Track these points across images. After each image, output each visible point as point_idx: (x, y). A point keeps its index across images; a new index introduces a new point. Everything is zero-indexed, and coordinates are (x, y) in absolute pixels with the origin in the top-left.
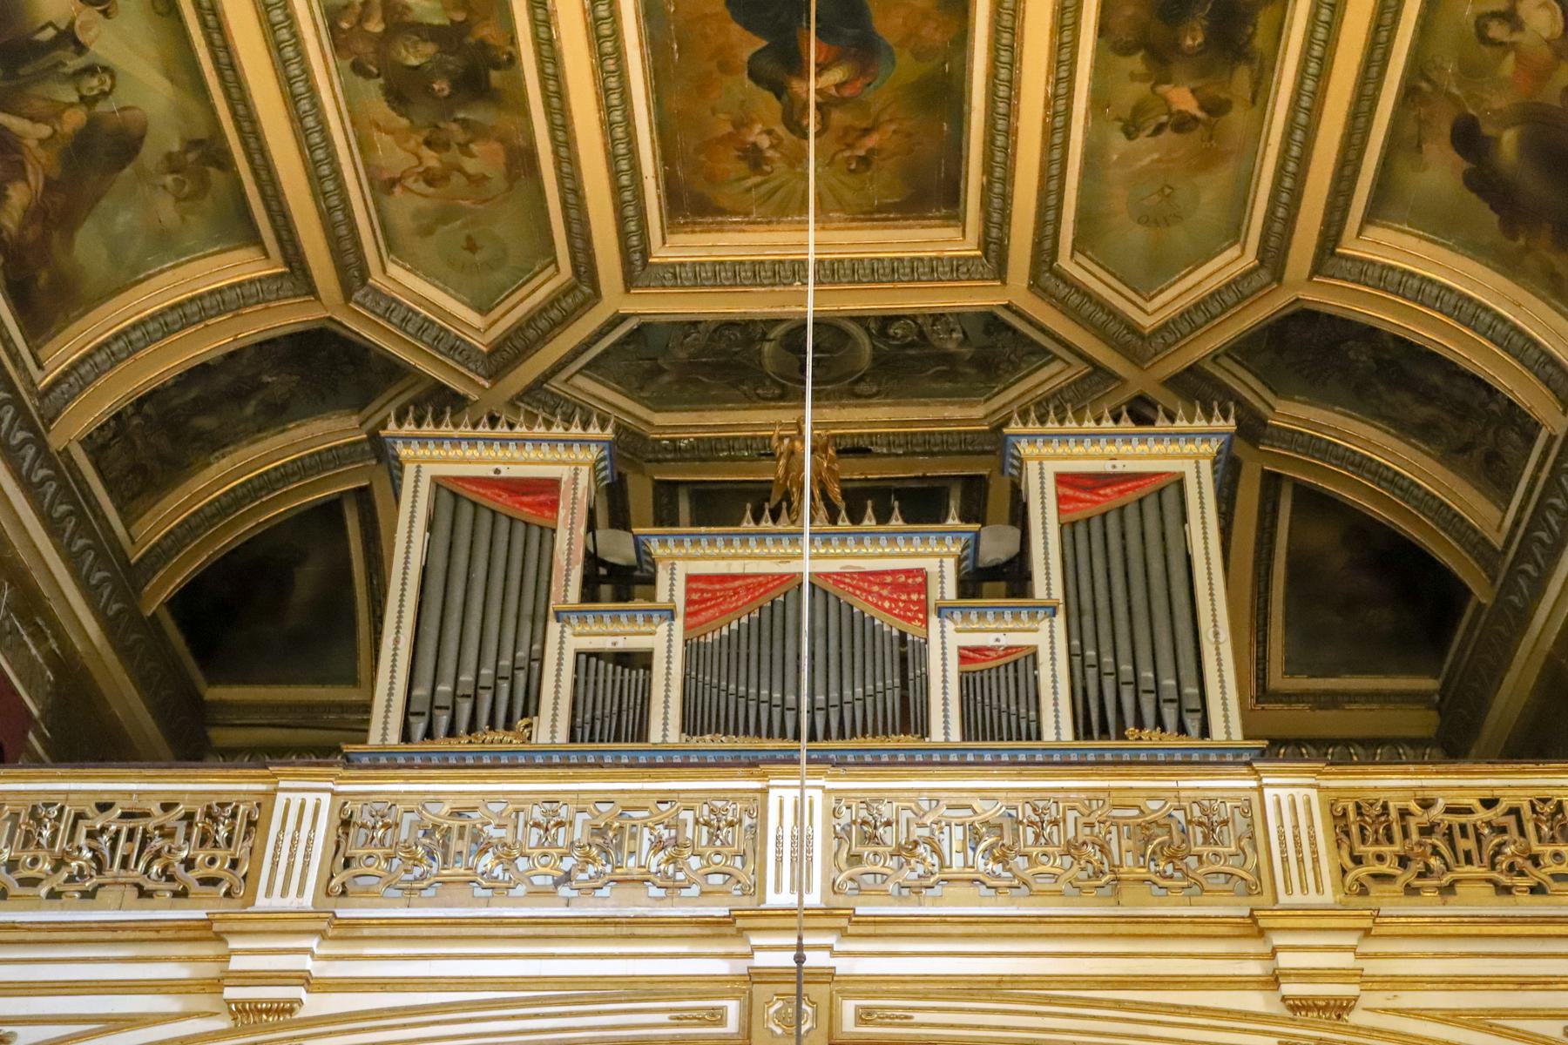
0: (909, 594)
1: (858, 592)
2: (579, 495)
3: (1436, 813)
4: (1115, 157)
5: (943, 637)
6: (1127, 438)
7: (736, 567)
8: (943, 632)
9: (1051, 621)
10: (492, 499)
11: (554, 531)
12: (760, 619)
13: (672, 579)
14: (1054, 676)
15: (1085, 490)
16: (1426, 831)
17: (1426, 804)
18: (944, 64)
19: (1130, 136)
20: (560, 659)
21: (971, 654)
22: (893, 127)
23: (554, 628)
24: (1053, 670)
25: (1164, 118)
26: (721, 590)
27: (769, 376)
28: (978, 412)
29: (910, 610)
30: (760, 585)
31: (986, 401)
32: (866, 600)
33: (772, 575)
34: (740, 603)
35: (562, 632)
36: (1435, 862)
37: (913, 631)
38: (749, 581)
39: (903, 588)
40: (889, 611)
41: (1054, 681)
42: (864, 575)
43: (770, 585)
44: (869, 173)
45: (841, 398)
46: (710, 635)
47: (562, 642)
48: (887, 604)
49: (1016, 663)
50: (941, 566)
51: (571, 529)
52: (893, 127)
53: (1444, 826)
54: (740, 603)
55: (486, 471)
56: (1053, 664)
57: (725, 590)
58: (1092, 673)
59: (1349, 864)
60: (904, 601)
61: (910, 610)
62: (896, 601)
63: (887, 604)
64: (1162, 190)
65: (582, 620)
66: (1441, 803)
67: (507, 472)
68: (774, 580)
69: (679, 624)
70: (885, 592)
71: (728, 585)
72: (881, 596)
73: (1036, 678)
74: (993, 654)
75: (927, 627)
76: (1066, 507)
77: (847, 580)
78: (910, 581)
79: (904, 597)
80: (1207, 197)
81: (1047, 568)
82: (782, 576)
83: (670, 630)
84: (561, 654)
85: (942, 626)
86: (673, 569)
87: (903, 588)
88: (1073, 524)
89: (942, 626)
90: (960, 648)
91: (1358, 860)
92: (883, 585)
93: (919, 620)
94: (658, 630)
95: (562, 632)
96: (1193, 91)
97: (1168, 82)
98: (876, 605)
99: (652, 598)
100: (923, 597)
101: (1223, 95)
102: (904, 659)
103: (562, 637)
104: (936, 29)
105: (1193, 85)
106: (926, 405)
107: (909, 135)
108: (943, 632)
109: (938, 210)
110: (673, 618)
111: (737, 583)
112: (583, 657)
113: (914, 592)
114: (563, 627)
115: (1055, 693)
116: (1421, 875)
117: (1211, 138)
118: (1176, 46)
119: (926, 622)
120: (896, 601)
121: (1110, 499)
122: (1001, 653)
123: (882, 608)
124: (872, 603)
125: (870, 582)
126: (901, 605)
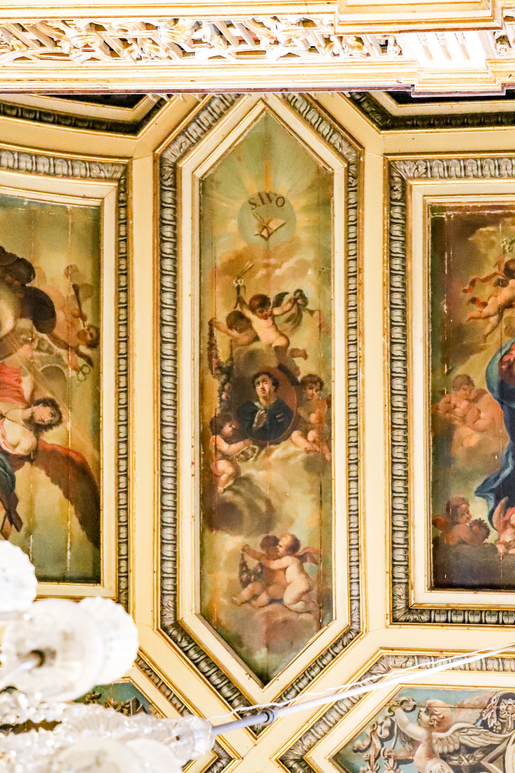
4: (310, 272)
18: (449, 373)
19: (300, 294)
22: (486, 310)
25: (277, 311)
44: (507, 259)
52: (486, 310)
64: (269, 235)
80: (233, 225)
96: (257, 338)
97: (277, 348)
101: (235, 333)
104: (455, 407)
105: (256, 346)
107: (474, 300)
109: (449, 217)
117: (238, 288)
118: (276, 384)
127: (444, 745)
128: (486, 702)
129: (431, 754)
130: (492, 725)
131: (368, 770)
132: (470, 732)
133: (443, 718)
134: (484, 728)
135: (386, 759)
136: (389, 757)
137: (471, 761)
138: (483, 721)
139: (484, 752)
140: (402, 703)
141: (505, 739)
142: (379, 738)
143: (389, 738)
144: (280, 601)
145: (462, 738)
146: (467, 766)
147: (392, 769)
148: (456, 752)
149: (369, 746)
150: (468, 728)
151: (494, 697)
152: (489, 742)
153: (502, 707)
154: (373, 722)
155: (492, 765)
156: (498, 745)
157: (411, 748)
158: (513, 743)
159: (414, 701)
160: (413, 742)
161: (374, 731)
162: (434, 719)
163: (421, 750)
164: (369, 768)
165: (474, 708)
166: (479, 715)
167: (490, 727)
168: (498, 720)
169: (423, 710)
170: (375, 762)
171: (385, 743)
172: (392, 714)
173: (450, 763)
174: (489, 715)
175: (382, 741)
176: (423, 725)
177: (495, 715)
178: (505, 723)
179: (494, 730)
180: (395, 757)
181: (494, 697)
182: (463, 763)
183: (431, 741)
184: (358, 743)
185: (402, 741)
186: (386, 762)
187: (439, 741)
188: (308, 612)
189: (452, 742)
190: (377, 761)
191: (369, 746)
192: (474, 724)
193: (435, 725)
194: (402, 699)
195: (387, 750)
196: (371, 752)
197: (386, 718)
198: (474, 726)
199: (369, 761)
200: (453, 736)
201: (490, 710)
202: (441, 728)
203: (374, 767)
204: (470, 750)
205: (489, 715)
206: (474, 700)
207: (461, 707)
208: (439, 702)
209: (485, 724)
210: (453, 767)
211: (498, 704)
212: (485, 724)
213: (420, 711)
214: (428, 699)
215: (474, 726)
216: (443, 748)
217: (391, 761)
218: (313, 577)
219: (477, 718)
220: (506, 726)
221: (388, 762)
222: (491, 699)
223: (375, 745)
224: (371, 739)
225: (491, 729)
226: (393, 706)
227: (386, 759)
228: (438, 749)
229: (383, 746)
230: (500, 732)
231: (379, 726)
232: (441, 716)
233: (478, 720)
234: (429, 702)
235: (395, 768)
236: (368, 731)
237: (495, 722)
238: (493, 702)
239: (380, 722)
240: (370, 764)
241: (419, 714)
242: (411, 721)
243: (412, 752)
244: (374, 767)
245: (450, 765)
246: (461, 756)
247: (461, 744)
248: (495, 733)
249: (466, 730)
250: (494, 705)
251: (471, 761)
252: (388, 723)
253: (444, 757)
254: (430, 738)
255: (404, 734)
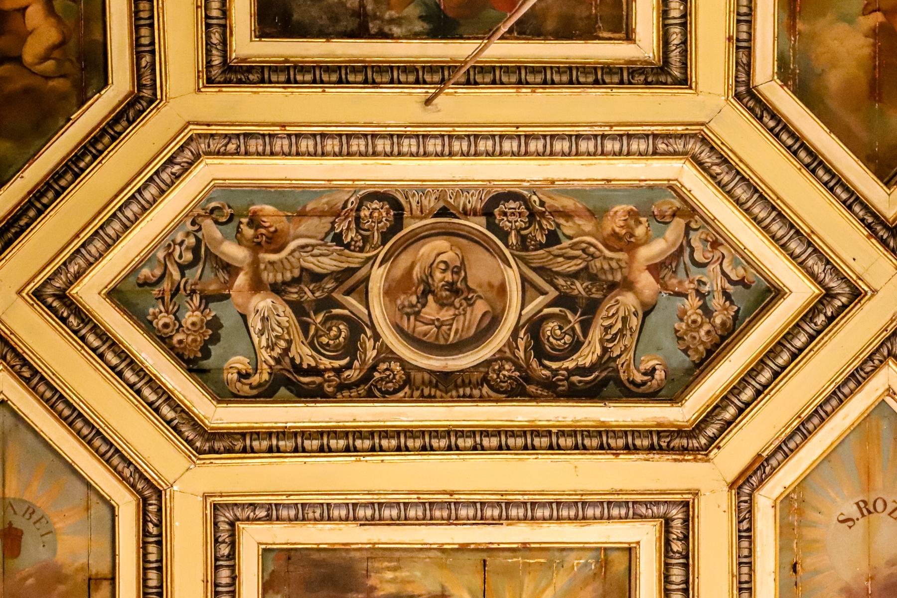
127: (277, 272)
128: (340, 205)
129: (257, 285)
130: (349, 240)
131: (161, 312)
132: (316, 251)
133: (276, 231)
134: (337, 245)
135: (189, 295)
136: (193, 292)
137: (317, 294)
138: (335, 234)
139: (336, 280)
140: (213, 210)
141: (369, 259)
142: (176, 262)
143: (193, 264)
144: (18, 60)
145: (304, 261)
146: (312, 301)
147: (198, 309)
148: (296, 281)
149: (163, 276)
150: (314, 246)
151: (352, 199)
152: (345, 265)
153: (365, 213)
154: (168, 240)
155: (349, 298)
156: (359, 268)
157: (227, 278)
158: (380, 266)
159: (230, 207)
160: (231, 270)
161: (170, 255)
162: (262, 234)
163: (242, 280)
164: (163, 309)
165: (321, 214)
166: (329, 226)
167: (345, 242)
168: (357, 232)
169: (245, 220)
170: (171, 300)
171: (187, 272)
172: (196, 228)
173: (285, 298)
174: (345, 225)
175: (182, 268)
176: (245, 242)
177: (353, 225)
178: (368, 236)
179: (352, 247)
180: (202, 291)
181: (352, 199)
182: (306, 297)
183: (258, 267)
184: (146, 272)
185: (212, 267)
186: (188, 299)
187: (269, 266)
188: (61, 76)
189: (288, 266)
190: (174, 300)
191: (163, 276)
192: (322, 240)
193: (263, 243)
194: (213, 204)
195: (190, 281)
196: (166, 285)
197: (188, 234)
198: (322, 242)
199: (162, 298)
200: (290, 257)
201: (346, 218)
202: (272, 247)
203: (171, 307)
204: (317, 278)
205: (345, 225)
206: (322, 203)
207: (303, 214)
208: (269, 209)
209: (338, 239)
210: (290, 303)
211: (358, 210)
212: (338, 239)
213: (241, 223)
214: (253, 204)
215: (320, 242)
216: (275, 276)
217: (196, 300)
218: (70, 23)
219: (326, 230)
220: (370, 240)
221: (192, 300)
222: (348, 200)
223: (171, 275)
224: (166, 266)
225: (348, 246)
226: (199, 215)
227: (189, 295)
228: (268, 277)
229: (183, 275)
230: (362, 250)
231: (177, 247)
232: (272, 229)
233: (327, 234)
234: (253, 208)
235: (202, 307)
236: (161, 254)
237: (353, 236)
238: (349, 206)
239: (179, 240)
240: (163, 305)
241: (239, 227)
242: (226, 237)
243: (229, 284)
244: (171, 307)
245: (286, 301)
246: (302, 286)
247: (303, 269)
248: (354, 251)
249: (309, 249)
250: (352, 210)
251: (317, 294)
252: (192, 240)
253: (277, 289)
254: (255, 263)
255: (216, 256)
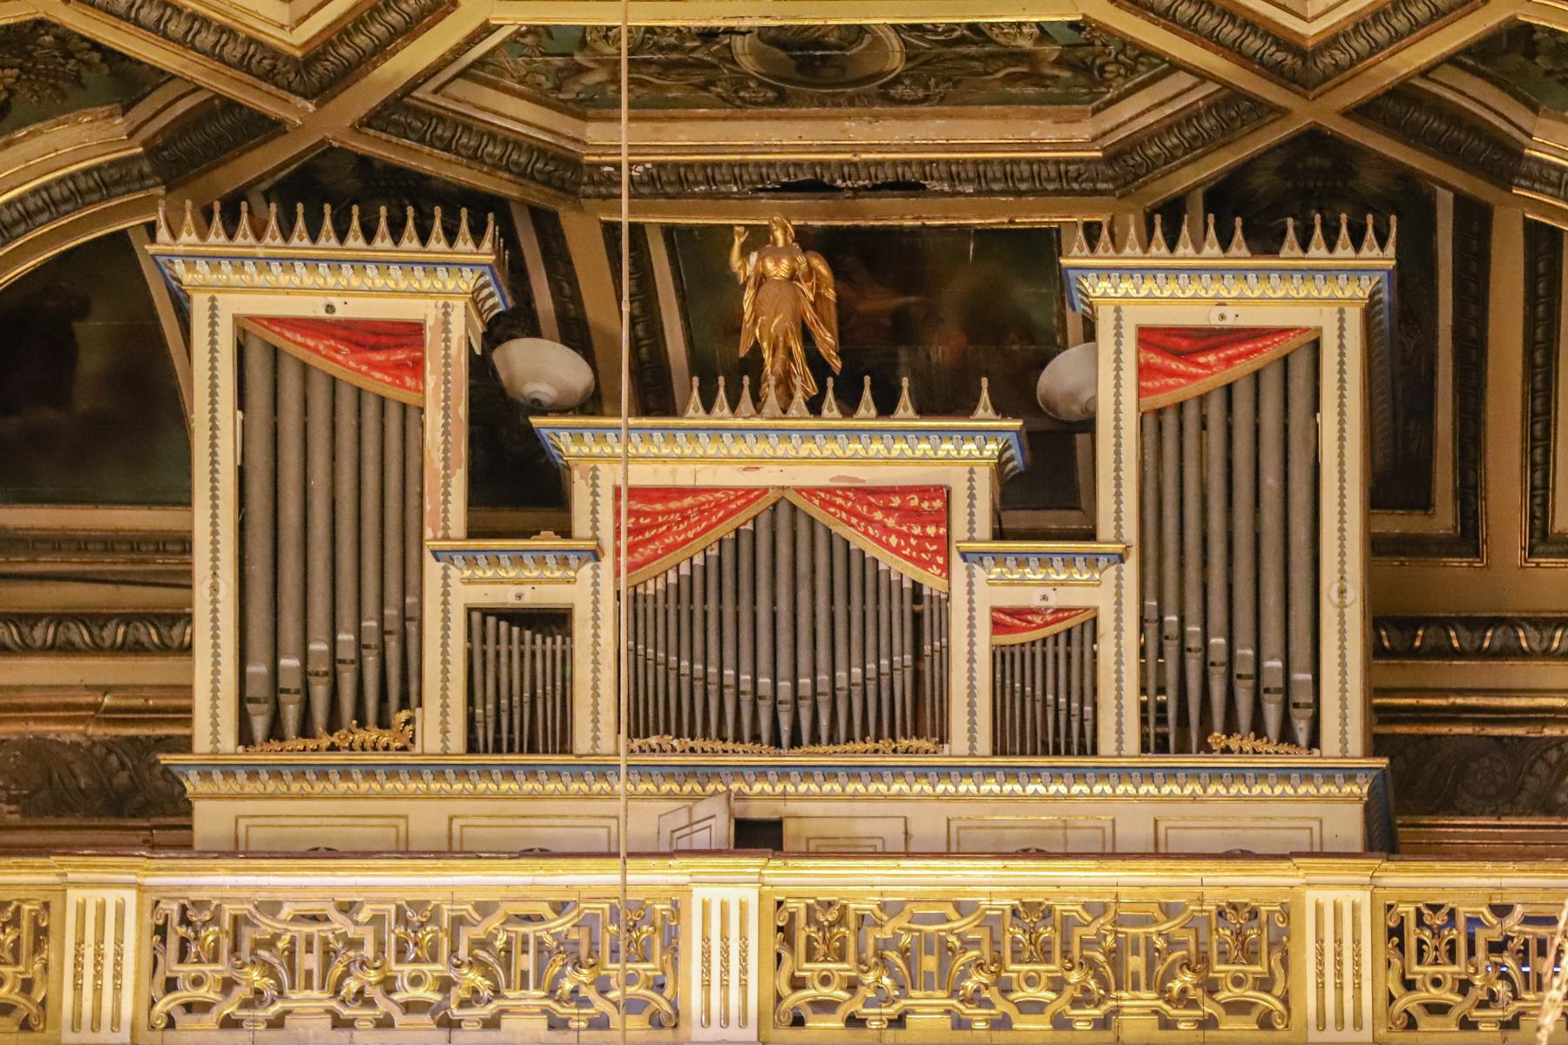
0: (923, 527)
1: (854, 521)
2: (453, 351)
3: (1512, 923)
5: (970, 592)
6: (1241, 273)
7: (683, 476)
8: (970, 584)
9: (1119, 571)
10: (326, 357)
11: (422, 410)
12: (720, 558)
13: (595, 494)
14: (1119, 654)
15: (1178, 355)
16: (1496, 948)
17: (1502, 911)
20: (446, 619)
21: (1008, 619)
23: (433, 569)
24: (1118, 645)
26: (663, 513)
27: (753, 78)
28: (1083, 131)
29: (927, 551)
30: (719, 505)
31: (1096, 111)
32: (866, 533)
33: (736, 490)
34: (690, 534)
35: (446, 577)
36: (1501, 988)
37: (931, 581)
38: (702, 498)
39: (915, 515)
40: (897, 551)
41: (1119, 663)
42: (864, 492)
43: (733, 506)
45: (871, 104)
46: (651, 584)
47: (446, 594)
48: (893, 541)
49: (1069, 631)
50: (971, 480)
51: (446, 408)
53: (1517, 944)
54: (690, 534)
55: (312, 307)
56: (1118, 637)
57: (669, 512)
58: (1171, 648)
59: (1396, 988)
60: (917, 537)
61: (927, 551)
62: (907, 536)
63: (893, 541)
65: (472, 562)
66: (1519, 910)
67: (348, 309)
68: (738, 498)
69: (607, 563)
70: (891, 522)
71: (674, 505)
72: (888, 531)
73: (1095, 655)
74: (1038, 620)
75: (948, 578)
76: (1149, 384)
77: (839, 501)
78: (925, 505)
79: (917, 530)
81: (1118, 485)
82: (749, 491)
83: (596, 576)
84: (446, 612)
85: (971, 575)
86: (595, 477)
87: (915, 515)
88: (1159, 412)
89: (971, 575)
90: (995, 609)
91: (1409, 985)
92: (888, 510)
93: (939, 566)
94: (579, 575)
95: (446, 577)
98: (878, 541)
99: (566, 533)
100: (942, 531)
102: (917, 618)
103: (446, 585)
106: (1005, 117)
108: (970, 584)
110: (597, 559)
111: (688, 501)
112: (476, 616)
113: (932, 523)
114: (445, 569)
115: (1119, 680)
116: (1482, 1005)
119: (946, 568)
120: (907, 536)
121: (1212, 373)
122: (1049, 618)
123: (887, 546)
124: (873, 538)
125: (870, 504)
126: (913, 542)
